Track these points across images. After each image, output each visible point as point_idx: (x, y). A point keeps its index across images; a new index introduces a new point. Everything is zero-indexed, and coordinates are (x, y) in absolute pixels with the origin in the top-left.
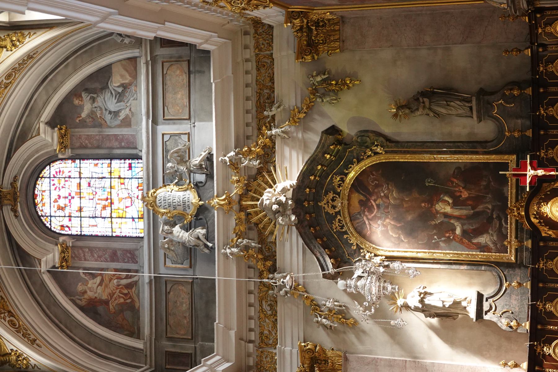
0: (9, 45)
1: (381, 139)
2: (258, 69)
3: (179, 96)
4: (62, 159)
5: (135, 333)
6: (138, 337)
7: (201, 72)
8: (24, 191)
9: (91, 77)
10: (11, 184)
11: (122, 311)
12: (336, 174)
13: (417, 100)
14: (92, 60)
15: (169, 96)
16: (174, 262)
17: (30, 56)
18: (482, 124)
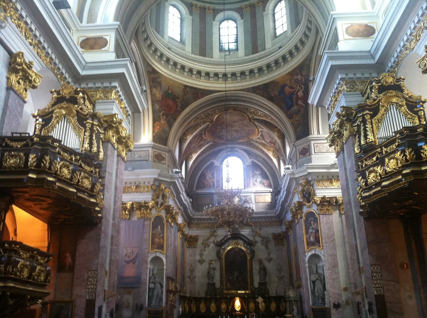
0: (274, 154)
3: (262, 199)
17: (271, 159)
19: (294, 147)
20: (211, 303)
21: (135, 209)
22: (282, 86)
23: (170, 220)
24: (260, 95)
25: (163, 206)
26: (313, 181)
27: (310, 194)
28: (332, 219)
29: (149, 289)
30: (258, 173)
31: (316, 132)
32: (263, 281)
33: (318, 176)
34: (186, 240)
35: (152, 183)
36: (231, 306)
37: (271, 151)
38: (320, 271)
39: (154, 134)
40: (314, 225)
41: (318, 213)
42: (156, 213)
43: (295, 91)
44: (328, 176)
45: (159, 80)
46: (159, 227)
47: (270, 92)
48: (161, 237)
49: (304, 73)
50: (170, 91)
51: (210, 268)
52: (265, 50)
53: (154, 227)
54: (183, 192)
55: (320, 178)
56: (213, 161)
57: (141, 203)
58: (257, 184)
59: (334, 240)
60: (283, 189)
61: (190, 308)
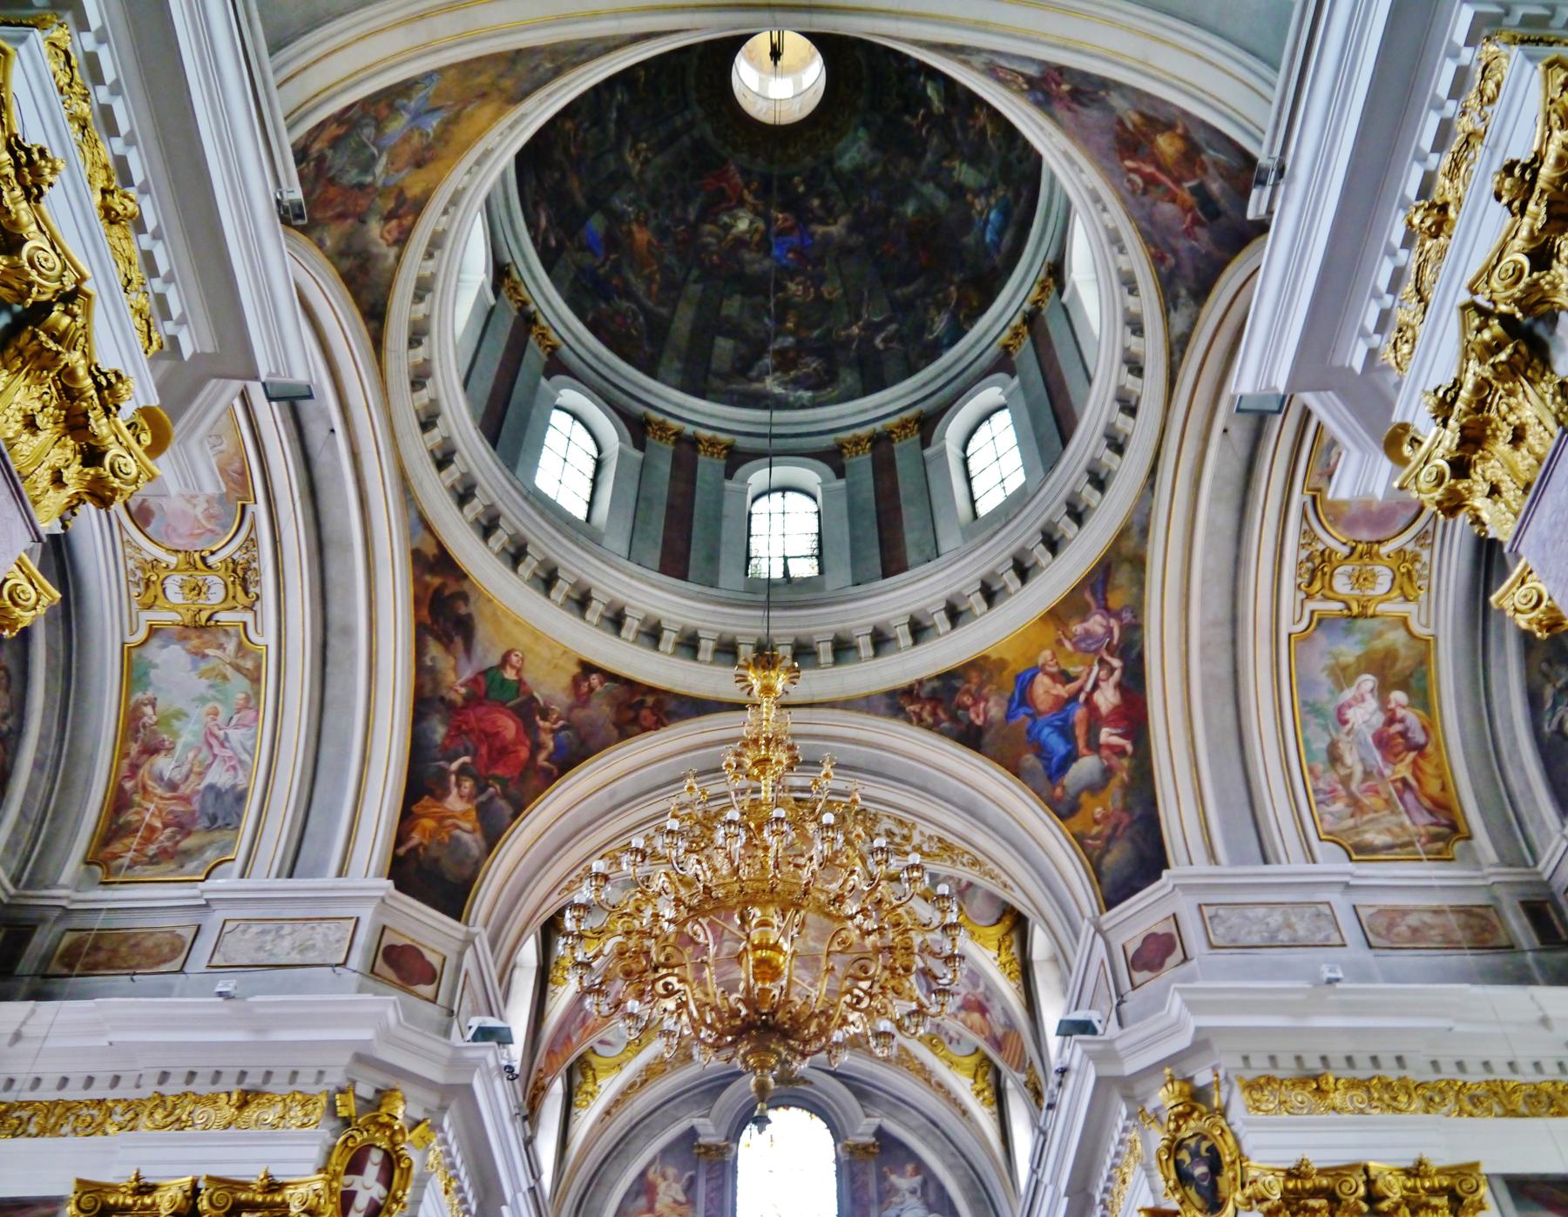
0: (979, 1087)
4: (835, 1145)
8: (793, 1093)
9: (941, 1188)
10: (802, 1078)
17: (965, 1112)
19: (1099, 940)
22: (1017, 677)
24: (920, 722)
26: (1225, 1088)
30: (904, 1182)
31: (1199, 854)
33: (1246, 1059)
35: (336, 1078)
37: (965, 1070)
39: (402, 851)
43: (1081, 689)
44: (1298, 1059)
45: (463, 610)
47: (967, 708)
49: (1116, 600)
50: (510, 674)
52: (938, 556)
54: (520, 1196)
55: (1260, 1066)
56: (695, 1121)
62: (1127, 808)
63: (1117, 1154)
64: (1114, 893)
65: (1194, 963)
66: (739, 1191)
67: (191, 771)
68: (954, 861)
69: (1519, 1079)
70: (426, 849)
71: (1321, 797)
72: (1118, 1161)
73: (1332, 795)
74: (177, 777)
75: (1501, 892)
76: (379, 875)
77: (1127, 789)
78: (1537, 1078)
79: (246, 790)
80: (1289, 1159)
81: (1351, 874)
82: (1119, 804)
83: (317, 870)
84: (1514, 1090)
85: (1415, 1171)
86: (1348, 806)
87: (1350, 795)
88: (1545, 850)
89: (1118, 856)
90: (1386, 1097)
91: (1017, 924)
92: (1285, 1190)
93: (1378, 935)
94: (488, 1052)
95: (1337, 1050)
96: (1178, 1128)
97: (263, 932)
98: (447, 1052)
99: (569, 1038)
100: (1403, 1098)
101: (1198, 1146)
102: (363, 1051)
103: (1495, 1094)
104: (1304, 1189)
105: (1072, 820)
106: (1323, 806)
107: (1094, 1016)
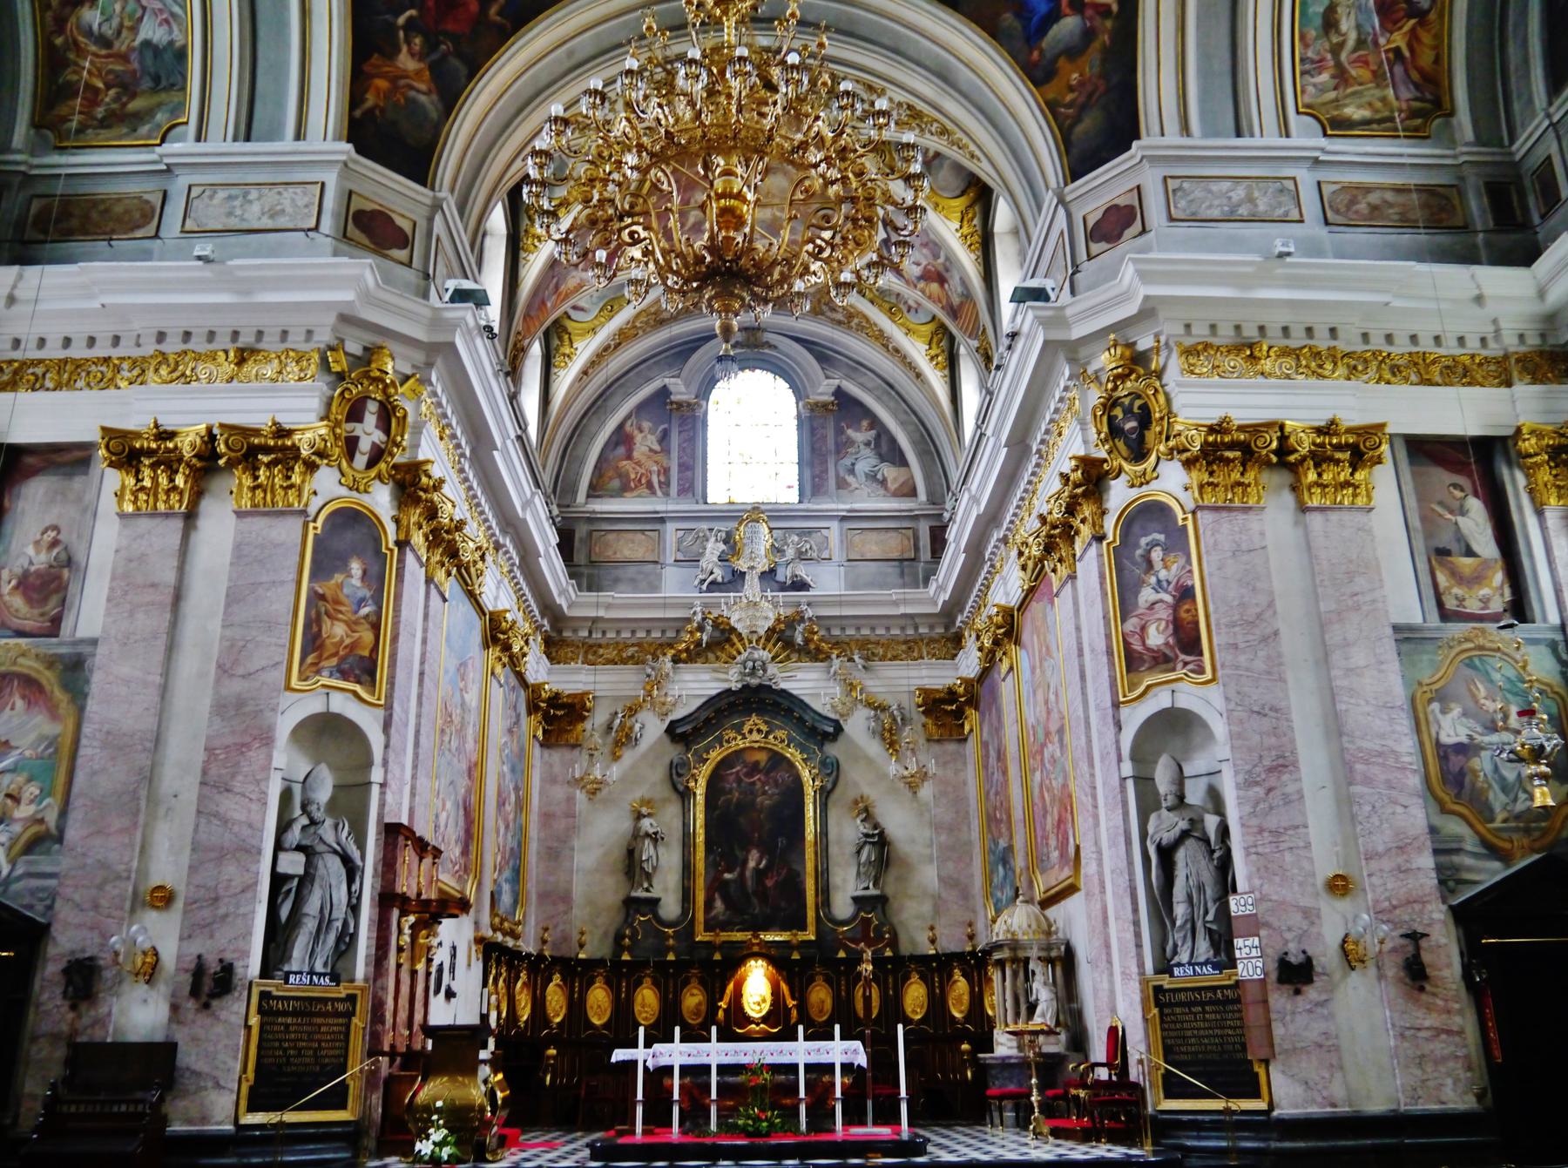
0: (933, 352)
1: (829, 786)
2: (906, 642)
3: (874, 548)
5: (595, 491)
6: (588, 496)
7: (902, 574)
9: (893, 441)
11: (620, 476)
12: (789, 736)
13: (875, 827)
14: (914, 443)
15: (873, 536)
16: (680, 541)
17: (919, 375)
18: (850, 901)
19: (1061, 212)
20: (639, 983)
21: (221, 462)
23: (418, 539)
25: (382, 466)
26: (1164, 354)
27: (1145, 418)
28: (1262, 534)
29: (278, 880)
30: (860, 436)
31: (1172, 124)
32: (873, 892)
33: (1188, 326)
34: (532, 708)
35: (324, 337)
36: (727, 998)
38: (1195, 794)
39: (358, 113)
40: (1166, 567)
41: (1190, 505)
42: (344, 491)
44: (1238, 328)
46: (356, 567)
48: (366, 617)
51: (637, 836)
53: (326, 560)
54: (509, 443)
55: (1200, 332)
57: (256, 432)
58: (855, 485)
59: (1276, 633)
60: (992, 441)
61: (539, 1004)
62: (1104, 75)
63: (1057, 411)
64: (1080, 163)
65: (1152, 234)
66: (709, 442)
67: (121, 25)
68: (922, 130)
69: (1442, 351)
70: (383, 111)
71: (1307, 67)
72: (1056, 417)
73: (1319, 66)
74: (108, 31)
75: (1468, 172)
76: (337, 138)
77: (1107, 53)
78: (1458, 351)
79: (185, 47)
80: (1213, 417)
81: (1322, 150)
82: (1096, 70)
83: (274, 134)
84: (1434, 362)
85: (1324, 430)
86: (1333, 77)
87: (1339, 65)
88: (1524, 126)
89: (1087, 125)
90: (1313, 364)
91: (980, 196)
92: (1206, 441)
93: (1337, 212)
94: (465, 311)
95: (1275, 321)
96: (1115, 388)
97: (230, 198)
98: (427, 313)
99: (543, 303)
100: (1329, 366)
101: (1132, 404)
102: (346, 312)
103: (1416, 364)
104: (1223, 443)
105: (1047, 86)
106: (1307, 77)
107: (1048, 284)
